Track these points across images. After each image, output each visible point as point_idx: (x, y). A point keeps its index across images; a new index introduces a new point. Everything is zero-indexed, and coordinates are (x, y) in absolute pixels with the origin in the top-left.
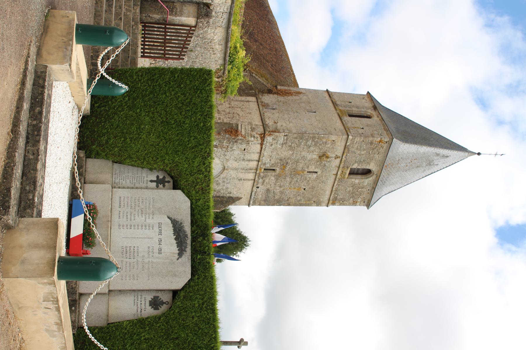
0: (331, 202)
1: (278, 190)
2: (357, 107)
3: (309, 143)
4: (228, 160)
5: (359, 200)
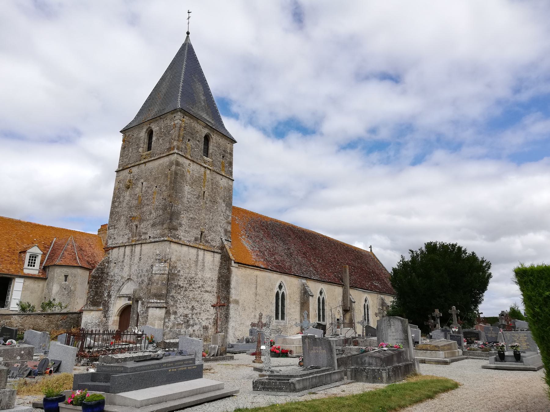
4: (122, 277)
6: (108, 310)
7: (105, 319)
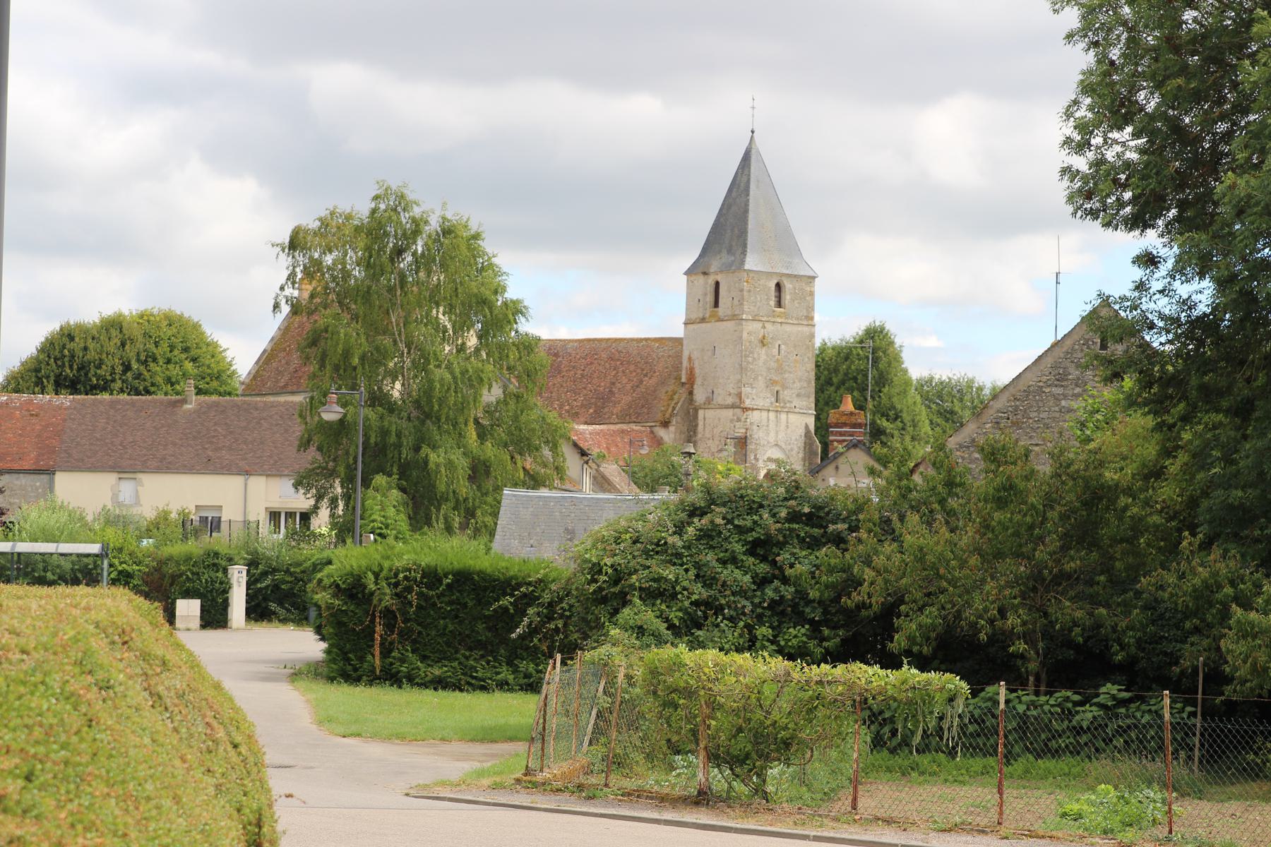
0: (810, 322)
1: (798, 385)
2: (706, 294)
3: (750, 359)
5: (808, 289)
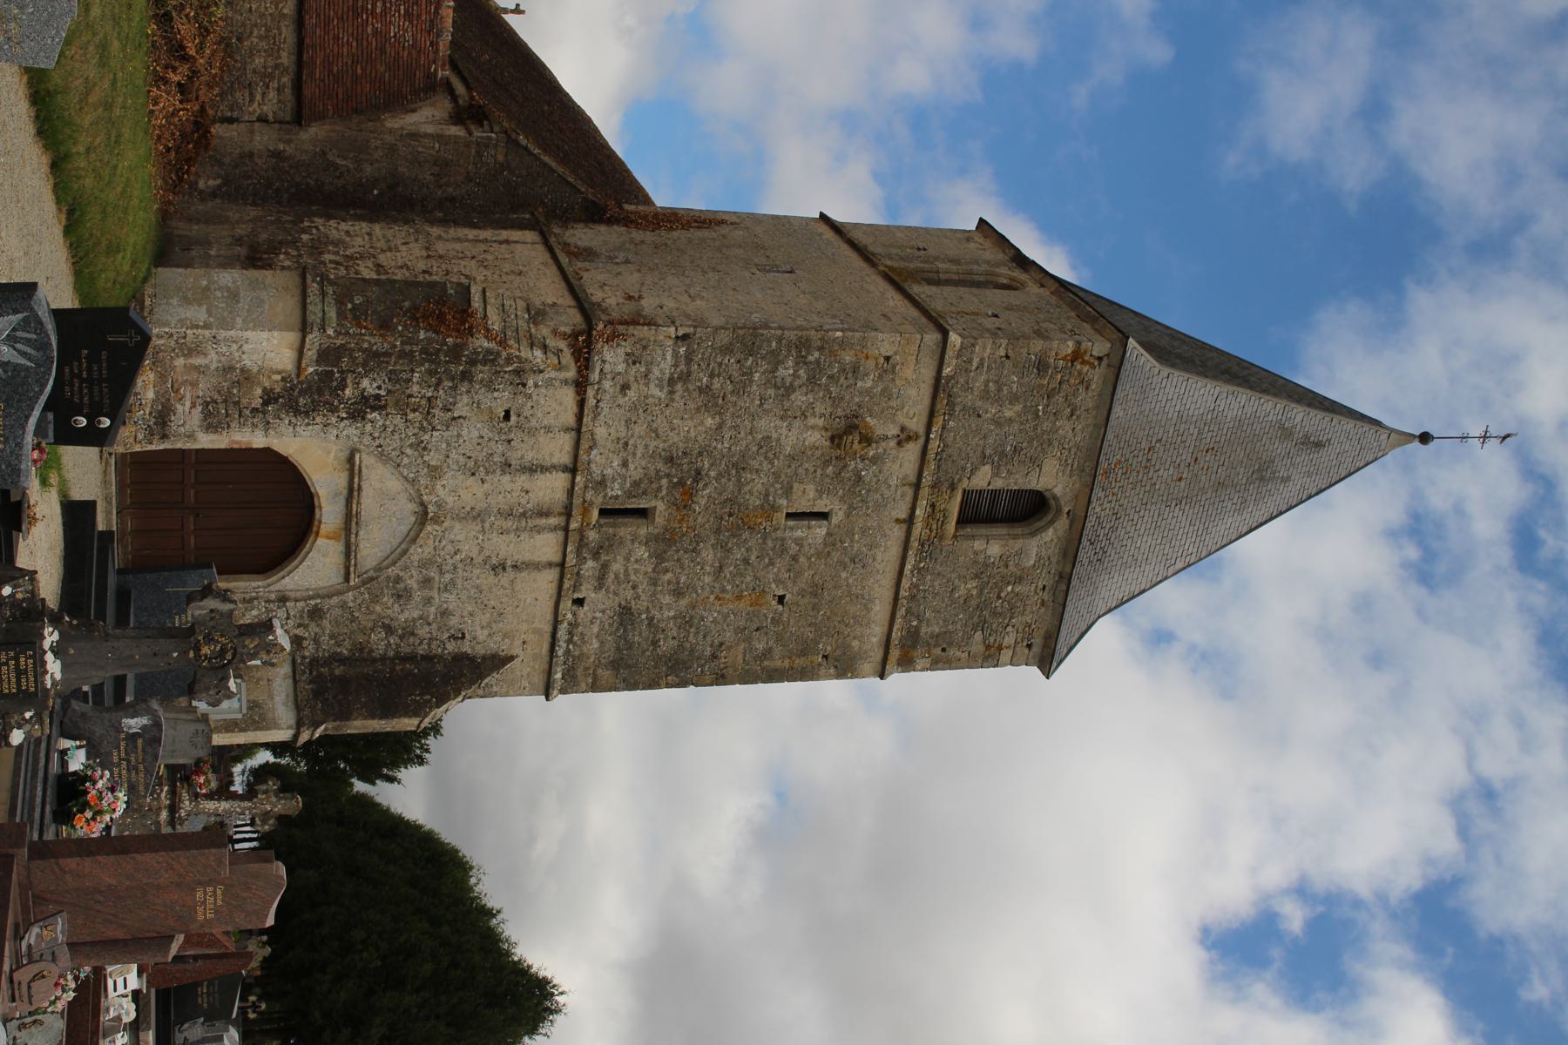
0: (895, 653)
1: (668, 609)
2: (956, 261)
3: (785, 372)
4: (435, 472)
5: (1009, 640)
6: (297, 412)
7: (257, 402)
